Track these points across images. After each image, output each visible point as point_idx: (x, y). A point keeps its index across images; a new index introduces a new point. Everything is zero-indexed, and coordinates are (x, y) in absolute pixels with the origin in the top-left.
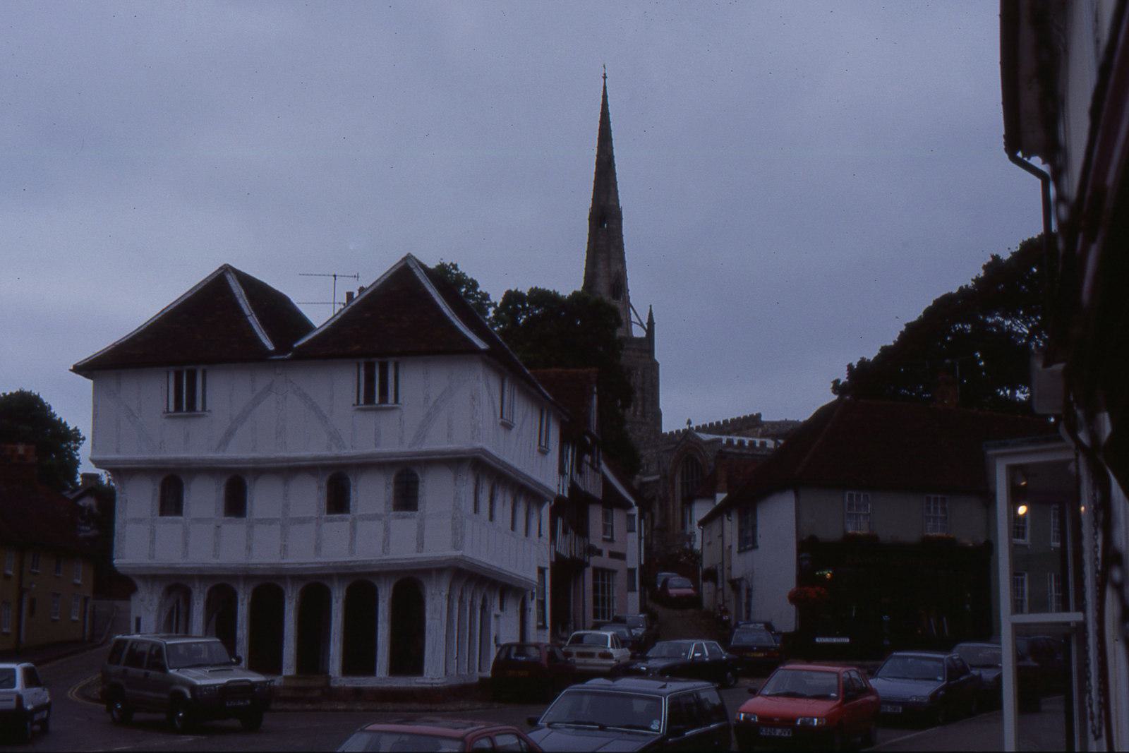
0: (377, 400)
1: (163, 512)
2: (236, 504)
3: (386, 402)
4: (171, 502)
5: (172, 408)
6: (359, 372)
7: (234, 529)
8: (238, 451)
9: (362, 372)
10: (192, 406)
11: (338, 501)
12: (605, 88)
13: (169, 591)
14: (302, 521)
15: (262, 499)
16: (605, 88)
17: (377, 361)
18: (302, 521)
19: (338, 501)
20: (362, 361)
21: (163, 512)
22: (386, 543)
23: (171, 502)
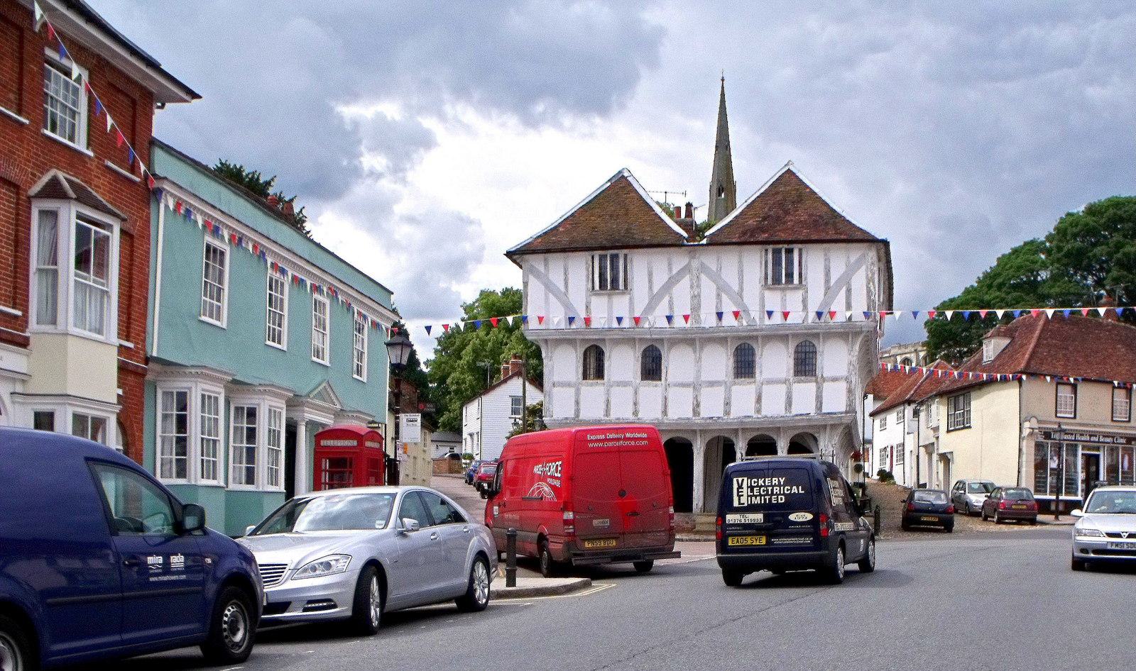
2: (652, 368)
3: (792, 282)
4: (594, 364)
5: (597, 287)
6: (766, 254)
7: (651, 392)
9: (770, 256)
10: (615, 281)
11: (745, 366)
14: (712, 384)
15: (676, 364)
18: (712, 384)
19: (745, 366)
21: (585, 377)
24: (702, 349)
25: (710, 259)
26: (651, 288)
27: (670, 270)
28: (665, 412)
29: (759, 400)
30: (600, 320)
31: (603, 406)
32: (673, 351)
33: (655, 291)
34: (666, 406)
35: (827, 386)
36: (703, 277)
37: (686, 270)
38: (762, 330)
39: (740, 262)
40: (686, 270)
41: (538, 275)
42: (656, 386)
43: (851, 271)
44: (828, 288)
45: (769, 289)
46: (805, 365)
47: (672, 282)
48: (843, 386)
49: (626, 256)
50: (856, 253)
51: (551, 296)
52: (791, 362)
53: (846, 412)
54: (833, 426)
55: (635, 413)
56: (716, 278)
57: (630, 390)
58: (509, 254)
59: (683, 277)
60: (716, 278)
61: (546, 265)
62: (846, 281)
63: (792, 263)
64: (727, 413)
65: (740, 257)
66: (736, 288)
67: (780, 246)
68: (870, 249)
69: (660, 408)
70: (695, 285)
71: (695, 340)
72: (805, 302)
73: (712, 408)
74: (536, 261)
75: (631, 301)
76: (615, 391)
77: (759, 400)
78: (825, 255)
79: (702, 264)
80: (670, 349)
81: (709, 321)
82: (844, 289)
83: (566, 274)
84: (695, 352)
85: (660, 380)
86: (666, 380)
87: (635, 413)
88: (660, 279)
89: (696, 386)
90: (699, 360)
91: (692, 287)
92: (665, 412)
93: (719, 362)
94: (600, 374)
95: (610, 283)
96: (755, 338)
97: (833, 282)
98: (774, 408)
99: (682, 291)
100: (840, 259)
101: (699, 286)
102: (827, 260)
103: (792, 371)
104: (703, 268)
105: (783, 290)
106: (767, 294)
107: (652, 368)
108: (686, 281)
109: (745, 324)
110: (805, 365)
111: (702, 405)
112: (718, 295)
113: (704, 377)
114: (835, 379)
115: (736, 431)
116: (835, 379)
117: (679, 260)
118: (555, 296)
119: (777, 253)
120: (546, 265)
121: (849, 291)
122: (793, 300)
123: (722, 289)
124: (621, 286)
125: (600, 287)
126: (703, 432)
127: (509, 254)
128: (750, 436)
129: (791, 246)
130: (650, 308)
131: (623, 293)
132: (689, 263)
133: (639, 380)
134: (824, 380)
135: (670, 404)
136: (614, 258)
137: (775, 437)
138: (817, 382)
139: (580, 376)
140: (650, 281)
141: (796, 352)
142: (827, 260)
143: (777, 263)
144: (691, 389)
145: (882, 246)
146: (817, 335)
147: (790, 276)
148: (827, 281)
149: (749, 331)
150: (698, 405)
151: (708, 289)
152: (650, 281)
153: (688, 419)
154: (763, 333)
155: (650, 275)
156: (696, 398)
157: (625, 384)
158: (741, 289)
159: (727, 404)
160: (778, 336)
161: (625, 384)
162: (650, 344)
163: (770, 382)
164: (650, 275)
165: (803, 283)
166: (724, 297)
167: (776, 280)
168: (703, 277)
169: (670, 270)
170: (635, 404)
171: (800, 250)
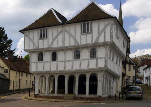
0: (86, 32)
1: (39, 60)
2: (54, 57)
3: (88, 32)
4: (41, 58)
5: (40, 38)
7: (54, 64)
8: (55, 45)
11: (77, 56)
13: (42, 76)
14: (69, 61)
15: (60, 56)
17: (86, 22)
18: (69, 61)
19: (77, 56)
20: (83, 23)
21: (39, 60)
22: (88, 65)
23: (41, 58)
24: (66, 51)
25: (67, 28)
26: (53, 37)
27: (57, 32)
28: (57, 69)
29: (81, 64)
30: (41, 47)
31: (43, 68)
32: (59, 53)
33: (54, 38)
34: (57, 67)
35: (99, 60)
36: (65, 33)
37: (61, 31)
38: (81, 46)
39: (75, 28)
40: (61, 31)
41: (27, 36)
42: (55, 62)
43: (105, 27)
44: (99, 33)
45: (82, 34)
46: (93, 54)
48: (104, 60)
50: (107, 22)
51: (30, 41)
52: (89, 54)
53: (105, 67)
54: (102, 71)
55: (50, 69)
56: (69, 33)
58: (20, 31)
59: (61, 33)
60: (69, 33)
61: (29, 33)
62: (104, 30)
63: (89, 27)
64: (72, 68)
65: (75, 27)
66: (74, 35)
67: (85, 22)
68: (111, 20)
69: (56, 67)
70: (64, 35)
71: (64, 49)
72: (92, 37)
73: (69, 67)
74: (27, 33)
75: (48, 40)
76: (46, 64)
77: (81, 64)
78: (98, 23)
79: (66, 30)
80: (58, 52)
81: (67, 44)
82: (103, 33)
83: (33, 35)
84: (64, 53)
85: (56, 60)
87: (50, 69)
88: (55, 34)
89: (65, 62)
90: (65, 55)
91: (63, 36)
92: (57, 69)
93: (70, 55)
95: (43, 36)
96: (80, 48)
97: (100, 30)
98: (84, 67)
99: (60, 37)
100: (102, 24)
101: (64, 35)
102: (99, 25)
103: (89, 57)
104: (66, 31)
105: (86, 34)
106: (82, 36)
107: (54, 57)
108: (61, 35)
109: (76, 44)
110: (93, 54)
111: (66, 67)
112: (69, 38)
113: (67, 59)
114: (101, 58)
115: (75, 73)
116: (101, 58)
117: (60, 29)
118: (31, 40)
119: (84, 24)
120: (29, 33)
121: (105, 33)
122: (89, 37)
123: (70, 35)
124: (45, 37)
125: (41, 38)
126: (67, 73)
127: (20, 31)
128: (79, 74)
129: (88, 22)
131: (46, 39)
132: (62, 29)
133: (51, 61)
134: (98, 58)
135: (58, 66)
137: (86, 74)
138: (96, 59)
139: (38, 60)
140: (53, 35)
141: (91, 51)
142: (99, 25)
143: (84, 27)
144: (63, 63)
145: (114, 19)
146: (96, 46)
147: (88, 30)
148: (99, 30)
149: (77, 46)
150: (65, 67)
151: (67, 35)
152: (53, 35)
154: (81, 46)
155: (53, 33)
156: (65, 65)
157: (48, 62)
158: (75, 35)
159: (72, 66)
160: (85, 47)
161: (48, 62)
162: (53, 51)
163: (84, 60)
164: (53, 33)
165: (92, 32)
166: (71, 37)
167: (84, 32)
168: (65, 33)
169: (57, 32)
170: (50, 67)
171: (91, 23)
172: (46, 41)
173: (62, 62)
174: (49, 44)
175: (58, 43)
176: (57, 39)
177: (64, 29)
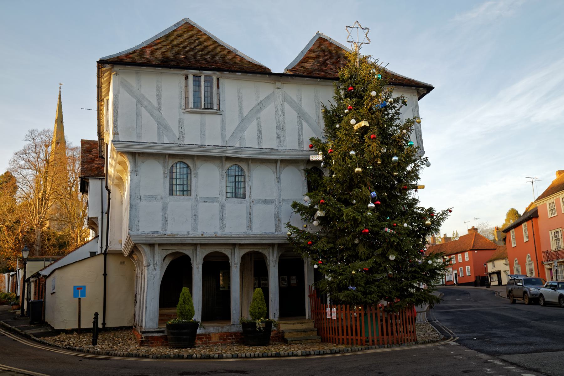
5: (191, 105)
12: (60, 92)
16: (60, 92)
21: (171, 192)
42: (241, 203)
47: (260, 107)
49: (218, 79)
57: (216, 206)
69: (245, 222)
86: (250, 197)
88: (249, 104)
92: (250, 226)
94: (186, 191)
124: (215, 107)
130: (241, 128)
136: (209, 80)
153: (273, 233)
155: (240, 98)
157: (213, 200)
161: (213, 200)
164: (240, 98)
172: (212, 121)
173: (266, 202)
174: (228, 135)
175: (260, 137)
176: (254, 123)
177: (279, 93)
